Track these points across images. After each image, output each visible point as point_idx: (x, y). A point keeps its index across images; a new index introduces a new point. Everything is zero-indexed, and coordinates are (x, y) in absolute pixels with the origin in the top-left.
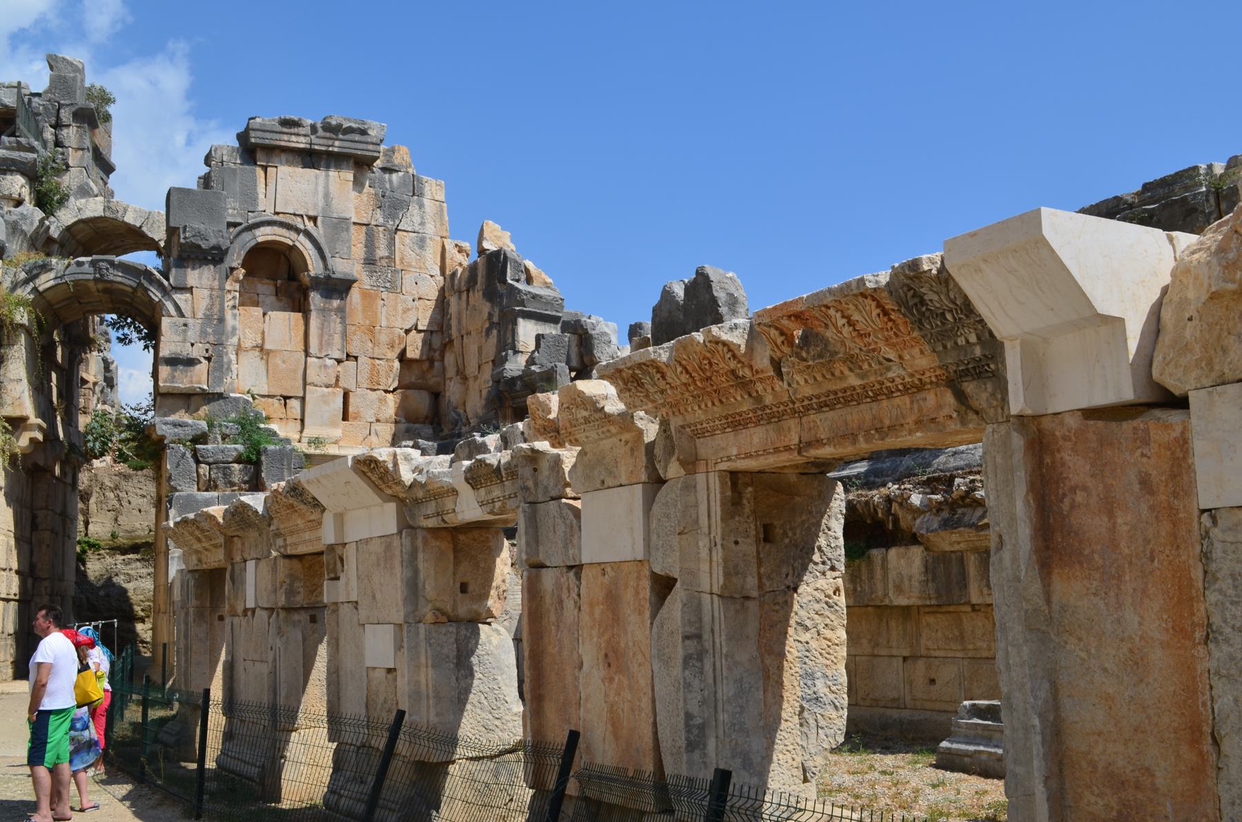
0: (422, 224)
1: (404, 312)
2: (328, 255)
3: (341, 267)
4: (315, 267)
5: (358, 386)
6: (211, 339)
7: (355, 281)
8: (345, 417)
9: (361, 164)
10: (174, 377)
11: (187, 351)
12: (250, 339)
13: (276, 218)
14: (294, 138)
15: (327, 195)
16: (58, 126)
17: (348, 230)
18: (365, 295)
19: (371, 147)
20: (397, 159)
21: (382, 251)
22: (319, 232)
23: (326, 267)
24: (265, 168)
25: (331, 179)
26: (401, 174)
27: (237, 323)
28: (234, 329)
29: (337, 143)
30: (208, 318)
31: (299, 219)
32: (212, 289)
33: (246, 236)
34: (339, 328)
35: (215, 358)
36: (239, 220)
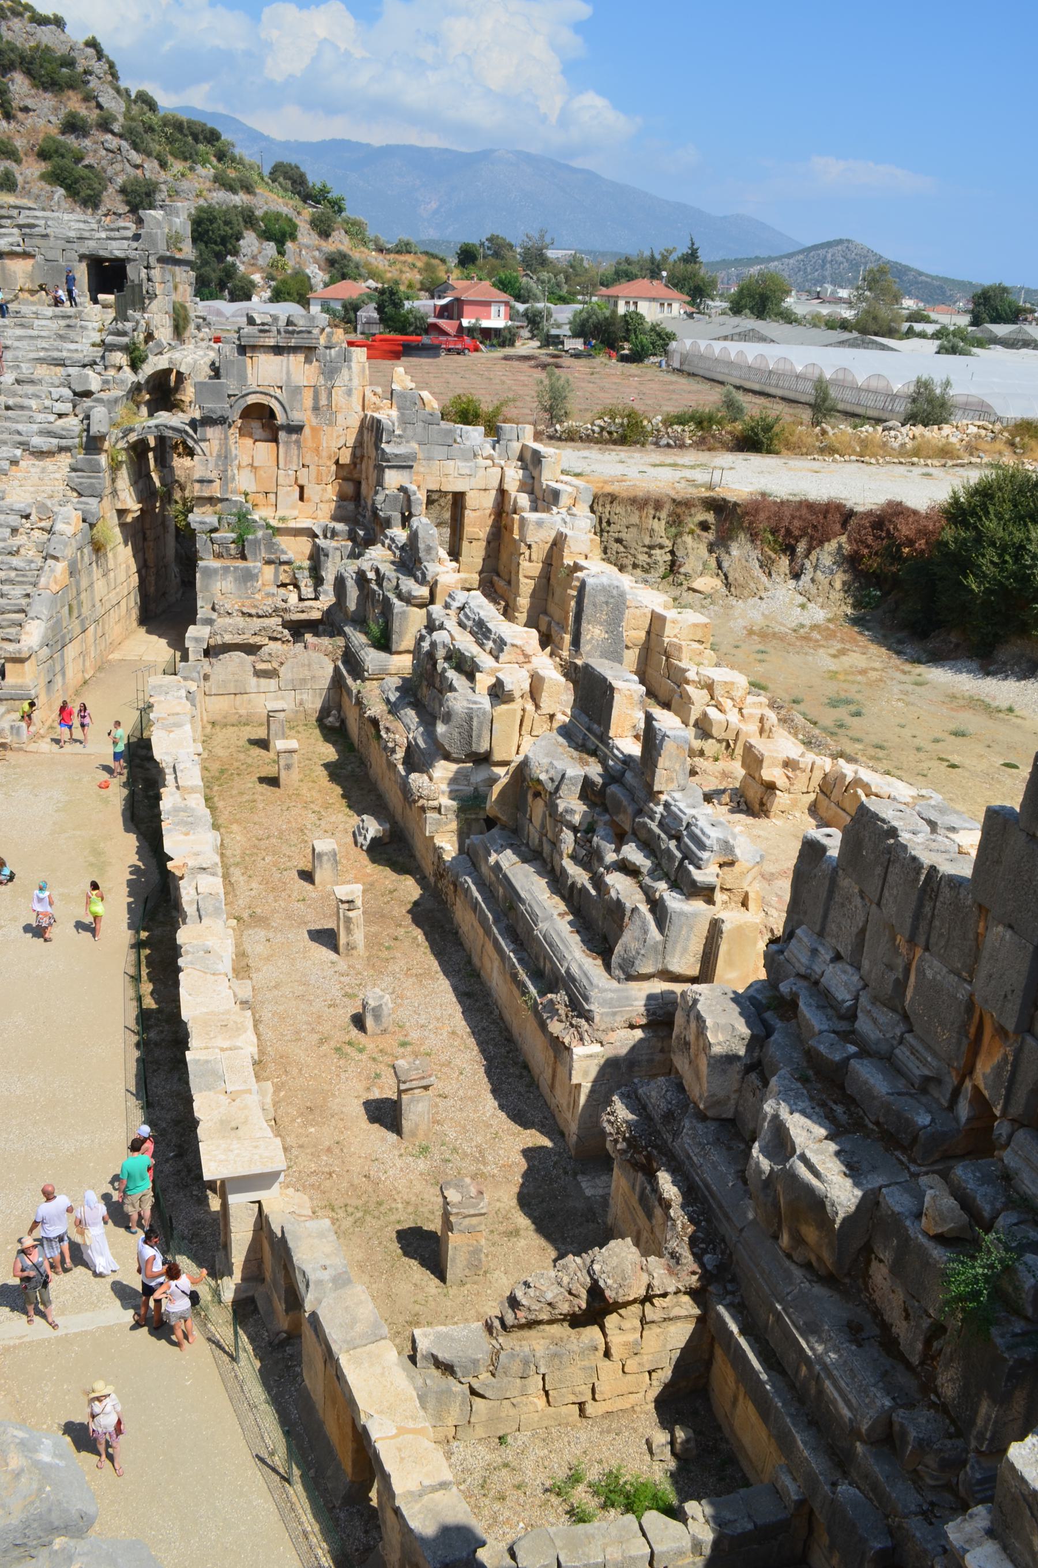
0: (350, 380)
3: (297, 416)
4: (281, 419)
8: (301, 498)
9: (309, 351)
12: (245, 460)
13: (258, 389)
15: (288, 373)
16: (148, 267)
18: (313, 429)
21: (323, 402)
30: (219, 456)
33: (241, 401)
35: (224, 479)
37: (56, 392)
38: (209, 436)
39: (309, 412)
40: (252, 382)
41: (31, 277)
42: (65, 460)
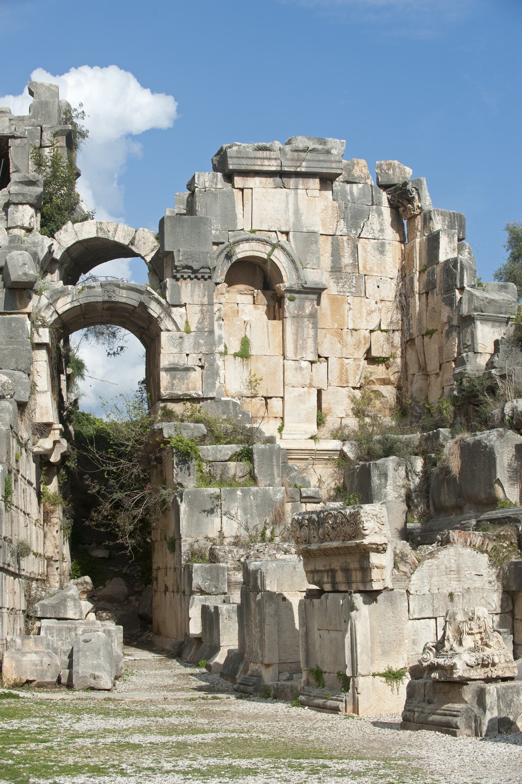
0: (382, 230)
1: (369, 314)
2: (300, 266)
3: (314, 276)
4: (289, 279)
5: (329, 385)
6: (204, 349)
7: (324, 289)
9: (327, 180)
10: (173, 385)
11: (184, 361)
13: (253, 235)
14: (266, 162)
15: (297, 212)
17: (316, 242)
18: (333, 300)
19: (334, 165)
20: (357, 172)
21: (347, 260)
22: (292, 246)
23: (299, 278)
24: (242, 190)
25: (300, 197)
26: (360, 186)
27: (223, 333)
28: (220, 338)
29: (304, 164)
30: (200, 331)
31: (273, 234)
32: (202, 305)
34: (311, 332)
36: (221, 240)
38: (185, 298)
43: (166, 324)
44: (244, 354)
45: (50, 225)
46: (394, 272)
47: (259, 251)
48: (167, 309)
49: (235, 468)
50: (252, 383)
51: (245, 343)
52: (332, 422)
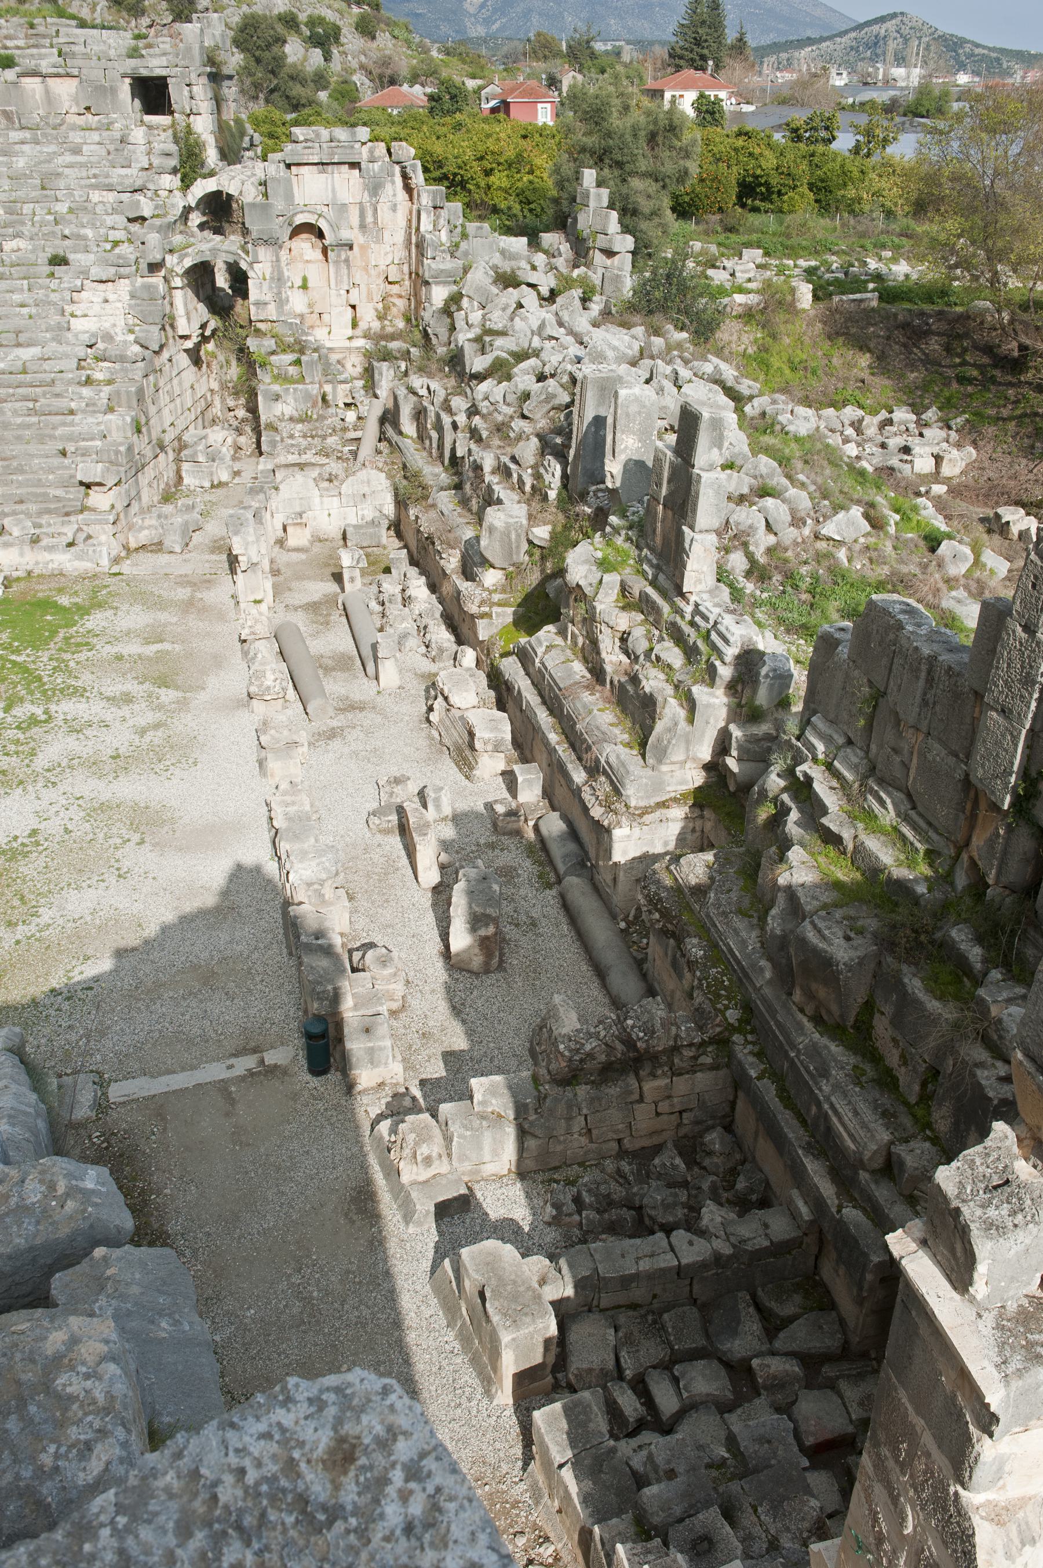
3: (346, 235)
4: (329, 239)
9: (355, 165)
15: (333, 190)
18: (362, 248)
21: (369, 219)
37: (109, 220)
39: (356, 230)
40: (298, 199)
41: (76, 100)
42: (124, 286)
43: (250, 274)
44: (304, 286)
45: (186, 183)
46: (402, 223)
47: (311, 219)
48: (251, 264)
49: (292, 370)
50: (310, 306)
51: (305, 280)
52: (363, 325)
